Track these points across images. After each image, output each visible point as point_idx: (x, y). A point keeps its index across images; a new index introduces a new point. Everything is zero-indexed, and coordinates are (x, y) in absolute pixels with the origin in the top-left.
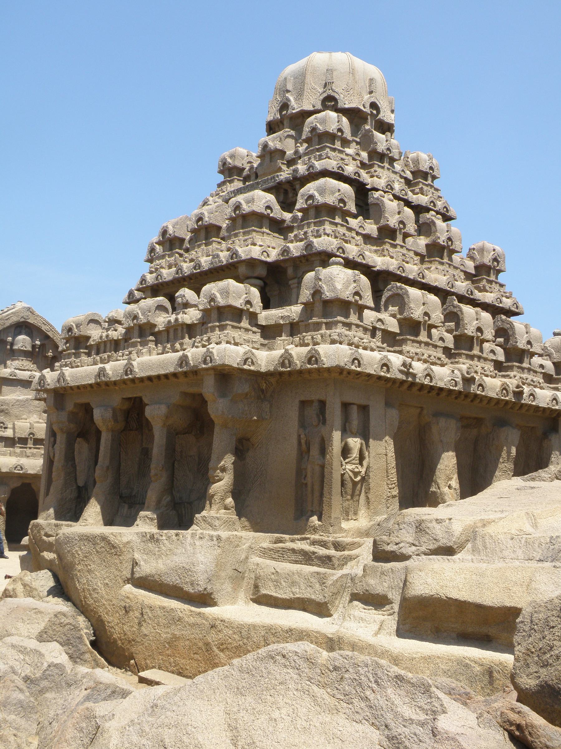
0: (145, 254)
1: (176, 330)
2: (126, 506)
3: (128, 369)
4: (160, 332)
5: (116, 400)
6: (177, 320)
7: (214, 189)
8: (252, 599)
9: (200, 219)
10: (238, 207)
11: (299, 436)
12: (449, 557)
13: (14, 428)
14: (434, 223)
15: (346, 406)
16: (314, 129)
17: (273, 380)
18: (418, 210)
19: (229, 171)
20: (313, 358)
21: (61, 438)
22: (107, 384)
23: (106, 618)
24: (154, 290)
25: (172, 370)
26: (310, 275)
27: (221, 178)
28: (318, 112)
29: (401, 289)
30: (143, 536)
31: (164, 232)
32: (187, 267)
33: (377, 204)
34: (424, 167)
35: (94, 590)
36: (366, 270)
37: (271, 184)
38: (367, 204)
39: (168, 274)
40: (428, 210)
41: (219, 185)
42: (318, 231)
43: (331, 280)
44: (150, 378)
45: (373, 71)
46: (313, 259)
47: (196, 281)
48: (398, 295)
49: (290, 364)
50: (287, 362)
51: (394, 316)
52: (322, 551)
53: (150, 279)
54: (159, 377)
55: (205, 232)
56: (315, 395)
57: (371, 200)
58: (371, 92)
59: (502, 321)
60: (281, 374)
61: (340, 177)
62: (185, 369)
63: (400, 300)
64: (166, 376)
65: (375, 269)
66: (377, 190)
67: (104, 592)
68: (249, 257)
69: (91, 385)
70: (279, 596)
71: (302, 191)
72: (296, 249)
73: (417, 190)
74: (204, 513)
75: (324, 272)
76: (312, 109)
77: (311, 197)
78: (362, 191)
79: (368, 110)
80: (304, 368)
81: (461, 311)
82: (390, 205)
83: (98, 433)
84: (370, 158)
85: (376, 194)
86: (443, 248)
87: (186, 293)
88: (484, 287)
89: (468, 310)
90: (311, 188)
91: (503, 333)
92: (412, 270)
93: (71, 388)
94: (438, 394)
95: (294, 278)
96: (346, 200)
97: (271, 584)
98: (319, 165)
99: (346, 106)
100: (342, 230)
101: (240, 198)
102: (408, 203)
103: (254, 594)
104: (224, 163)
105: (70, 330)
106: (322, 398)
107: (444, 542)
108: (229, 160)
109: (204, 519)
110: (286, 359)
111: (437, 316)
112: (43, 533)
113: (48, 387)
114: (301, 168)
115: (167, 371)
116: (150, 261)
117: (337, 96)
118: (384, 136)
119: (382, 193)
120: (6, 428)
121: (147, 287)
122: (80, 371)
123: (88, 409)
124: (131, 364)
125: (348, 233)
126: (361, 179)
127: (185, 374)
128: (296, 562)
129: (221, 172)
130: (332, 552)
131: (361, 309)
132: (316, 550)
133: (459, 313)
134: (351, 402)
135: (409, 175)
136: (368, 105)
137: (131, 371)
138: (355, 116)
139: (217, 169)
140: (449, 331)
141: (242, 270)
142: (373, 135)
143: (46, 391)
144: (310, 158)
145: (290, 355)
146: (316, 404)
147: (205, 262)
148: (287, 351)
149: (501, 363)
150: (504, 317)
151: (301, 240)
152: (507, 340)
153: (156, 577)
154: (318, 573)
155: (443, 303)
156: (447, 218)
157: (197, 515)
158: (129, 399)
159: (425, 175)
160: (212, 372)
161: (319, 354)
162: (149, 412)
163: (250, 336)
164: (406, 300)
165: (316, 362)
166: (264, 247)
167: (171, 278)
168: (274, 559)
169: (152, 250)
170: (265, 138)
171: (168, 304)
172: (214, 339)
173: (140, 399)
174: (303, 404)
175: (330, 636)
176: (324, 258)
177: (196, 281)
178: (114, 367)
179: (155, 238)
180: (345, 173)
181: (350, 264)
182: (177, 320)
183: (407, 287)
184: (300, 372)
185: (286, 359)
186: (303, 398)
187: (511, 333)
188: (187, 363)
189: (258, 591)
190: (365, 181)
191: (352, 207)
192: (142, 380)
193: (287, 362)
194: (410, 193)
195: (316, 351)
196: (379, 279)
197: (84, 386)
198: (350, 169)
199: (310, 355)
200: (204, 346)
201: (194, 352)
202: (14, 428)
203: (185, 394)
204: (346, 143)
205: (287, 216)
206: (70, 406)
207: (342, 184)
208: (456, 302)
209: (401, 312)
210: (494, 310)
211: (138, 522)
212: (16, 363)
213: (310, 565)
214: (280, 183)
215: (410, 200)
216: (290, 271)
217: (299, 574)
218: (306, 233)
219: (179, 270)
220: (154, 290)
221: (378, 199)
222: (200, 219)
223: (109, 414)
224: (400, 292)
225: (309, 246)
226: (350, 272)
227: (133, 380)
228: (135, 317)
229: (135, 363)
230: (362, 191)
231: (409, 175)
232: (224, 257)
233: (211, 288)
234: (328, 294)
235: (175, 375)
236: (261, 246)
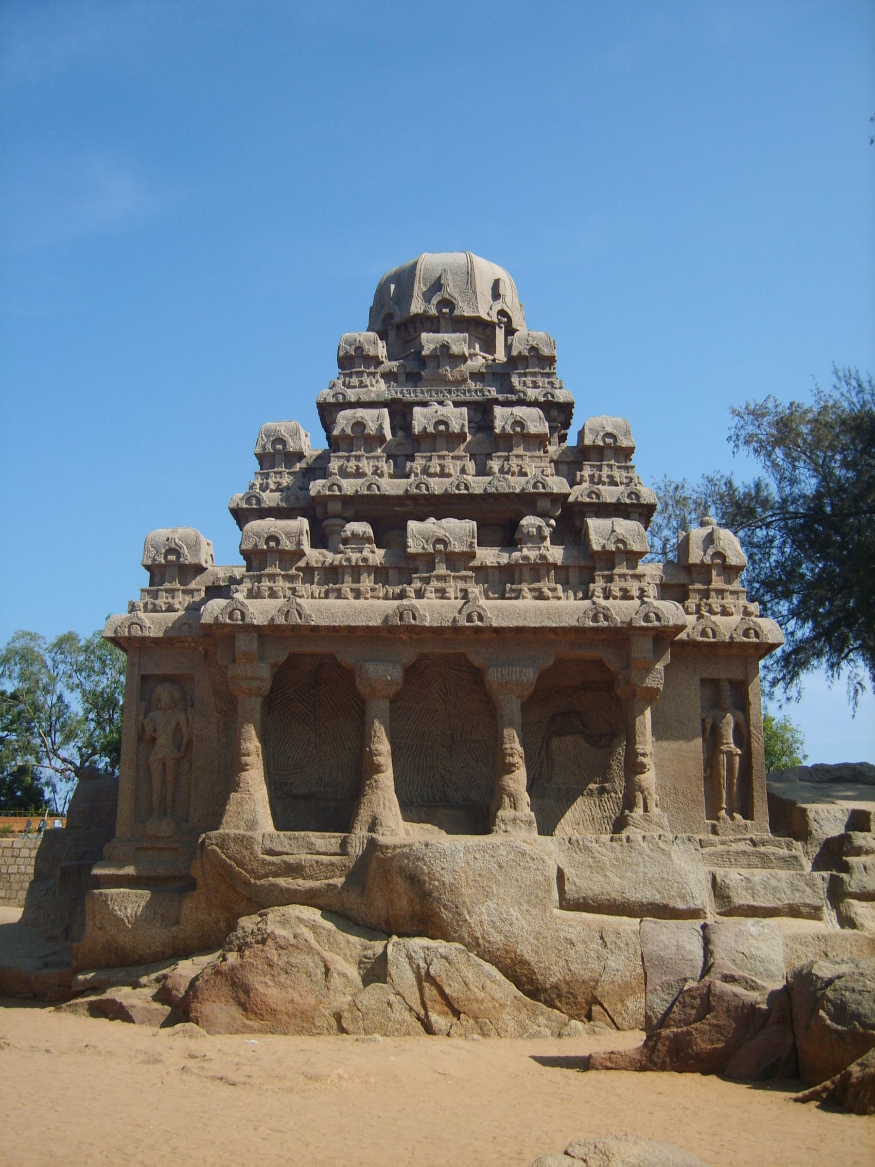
5: (409, 655)
8: (717, 913)
11: (703, 721)
25: (574, 623)
30: (560, 843)
46: (629, 510)
50: (710, 632)
56: (724, 672)
67: (523, 923)
80: (737, 640)
97: (744, 893)
112: (258, 850)
117: (511, 314)
146: (726, 686)
153: (615, 895)
174: (703, 681)
184: (731, 644)
186: (705, 675)
211: (500, 826)
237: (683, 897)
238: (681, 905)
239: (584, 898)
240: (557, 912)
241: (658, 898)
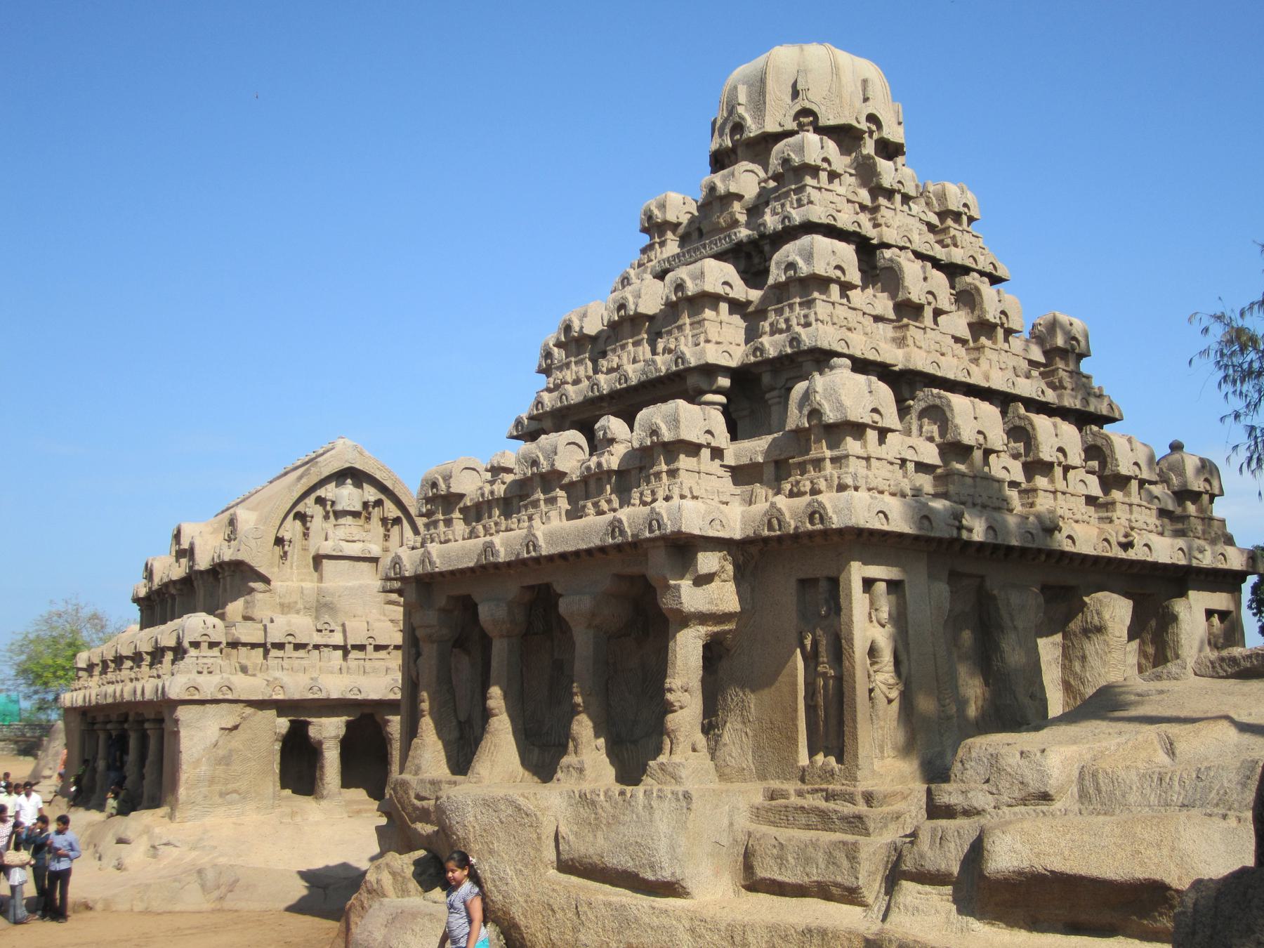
0: (536, 359)
1: (599, 479)
2: (536, 751)
3: (531, 542)
4: (572, 484)
5: (512, 589)
6: (599, 465)
7: (636, 257)
8: (743, 887)
9: (622, 306)
10: (680, 287)
12: (1045, 808)
13: (344, 632)
14: (977, 289)
15: (868, 584)
16: (786, 161)
17: (753, 550)
18: (953, 271)
19: (655, 228)
20: (816, 513)
21: (430, 652)
22: (497, 566)
23: (521, 921)
24: (560, 418)
25: (598, 542)
26: (800, 387)
27: (645, 240)
28: (791, 134)
29: (940, 397)
30: (570, 797)
31: (568, 328)
32: (605, 383)
33: (890, 269)
34: (954, 205)
35: (501, 879)
36: (883, 371)
37: (725, 245)
38: (875, 267)
39: (574, 394)
40: (966, 270)
41: (644, 251)
42: (806, 316)
43: (832, 393)
44: (563, 556)
45: (869, 69)
46: (800, 360)
47: (626, 403)
48: (935, 407)
49: (780, 525)
50: (775, 522)
51: (931, 439)
52: (847, 809)
53: (549, 400)
54: (577, 554)
55: (626, 325)
57: (881, 263)
58: (866, 100)
59: (1093, 434)
60: (766, 540)
61: (831, 231)
62: (619, 540)
63: (938, 414)
64: (589, 552)
65: (896, 368)
66: (888, 246)
68: (702, 362)
69: (472, 570)
70: (787, 880)
71: (776, 257)
72: (772, 345)
73: (949, 241)
74: (662, 759)
75: (820, 382)
76: (779, 129)
77: (791, 266)
78: (867, 249)
79: (864, 125)
81: (1031, 424)
82: (912, 270)
83: (486, 642)
84: (874, 197)
85: (888, 253)
86: (994, 326)
87: (613, 425)
88: (1060, 381)
89: (1042, 423)
90: (790, 251)
91: (1096, 452)
92: (953, 366)
93: (441, 574)
94: (1006, 555)
95: (773, 389)
96: (845, 267)
97: (772, 862)
98: (797, 216)
99: (831, 123)
100: (841, 312)
101: (683, 273)
102: (937, 264)
103: (745, 879)
104: (650, 217)
105: (434, 485)
106: (832, 574)
107: (1034, 786)
108: (656, 212)
109: (662, 767)
110: (774, 516)
111: (997, 437)
112: (412, 795)
113: (407, 574)
114: (771, 221)
115: (592, 545)
116: (546, 371)
118: (890, 163)
119: (897, 250)
120: (332, 631)
121: (546, 413)
122: (455, 548)
123: (468, 606)
124: (534, 535)
125: (850, 314)
126: (864, 232)
127: (618, 547)
128: (808, 827)
129: (645, 230)
130: (862, 808)
131: (883, 433)
132: (837, 808)
133: (1029, 428)
134: (877, 576)
135: (934, 220)
136: (863, 119)
137: (534, 546)
138: (845, 136)
139: (639, 227)
140: (1016, 456)
141: (692, 381)
142: (875, 164)
143: (403, 579)
144: (783, 206)
145: (779, 510)
146: (823, 585)
147: (633, 373)
148: (773, 505)
149: (1097, 498)
150: (1095, 428)
151: (781, 331)
152: (1103, 464)
153: (596, 859)
154: (844, 843)
155: (1004, 413)
156: (995, 280)
157: (651, 763)
158: (531, 588)
159: (957, 216)
160: (661, 543)
161: (824, 508)
162: (565, 606)
163: (714, 483)
164: (949, 414)
165: (822, 519)
166: (722, 342)
167: (581, 398)
168: (773, 824)
169: (548, 355)
170: (708, 177)
171: (582, 440)
172: (661, 494)
173: (548, 586)
174: (806, 584)
175: (871, 937)
176: (822, 358)
177: (626, 403)
178: (505, 541)
179: (551, 335)
180: (839, 225)
181: (861, 366)
182: (599, 465)
183: (949, 394)
184: (797, 537)
185: (774, 516)
186: (802, 576)
187: (1108, 452)
188: (622, 532)
189: (753, 873)
190: (868, 235)
191: (854, 276)
192: (550, 558)
193: (775, 522)
194: (937, 247)
195: (820, 503)
196: (904, 383)
197: (462, 572)
198: (845, 220)
199: (810, 510)
200: (644, 504)
201: (631, 516)
202: (344, 632)
203: (619, 577)
204: (833, 176)
205: (755, 295)
206: (442, 601)
207: (836, 242)
208: (1022, 410)
209: (943, 432)
210: (1082, 419)
211: (559, 774)
212: (341, 532)
213: (831, 830)
214: (740, 245)
215: (938, 257)
216: (766, 379)
217: (815, 844)
218: (787, 321)
219: (594, 385)
220: (560, 418)
221: (891, 260)
222: (622, 306)
223: (501, 612)
224: (938, 402)
225: (795, 340)
226: (861, 378)
227: (537, 560)
228: (535, 463)
229: (539, 534)
230: (867, 249)
231: (934, 220)
232: (663, 364)
233: (651, 415)
234: (831, 415)
235: (602, 550)
236: (718, 343)
237: (652, 867)
238: (650, 876)
239: (572, 860)
240: (553, 872)
241: (630, 865)
